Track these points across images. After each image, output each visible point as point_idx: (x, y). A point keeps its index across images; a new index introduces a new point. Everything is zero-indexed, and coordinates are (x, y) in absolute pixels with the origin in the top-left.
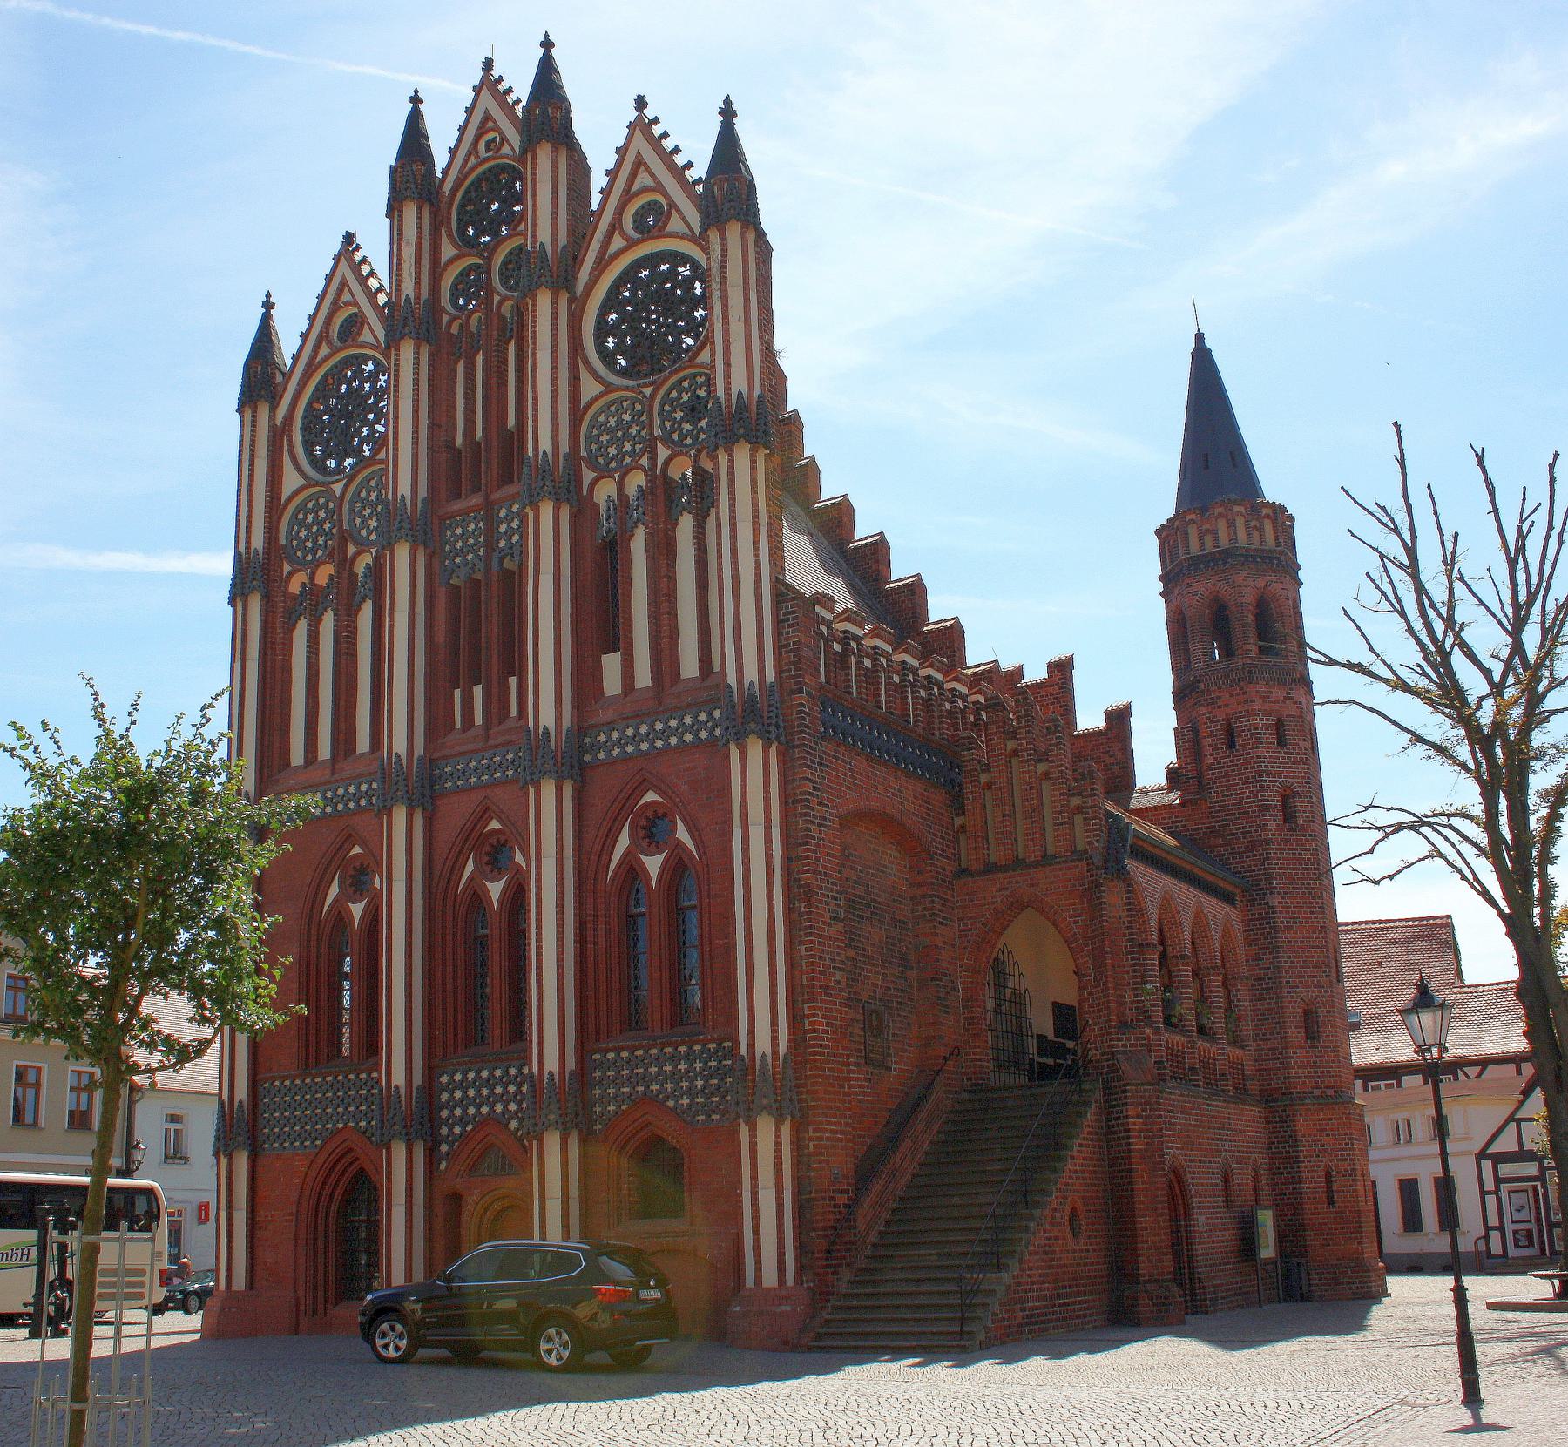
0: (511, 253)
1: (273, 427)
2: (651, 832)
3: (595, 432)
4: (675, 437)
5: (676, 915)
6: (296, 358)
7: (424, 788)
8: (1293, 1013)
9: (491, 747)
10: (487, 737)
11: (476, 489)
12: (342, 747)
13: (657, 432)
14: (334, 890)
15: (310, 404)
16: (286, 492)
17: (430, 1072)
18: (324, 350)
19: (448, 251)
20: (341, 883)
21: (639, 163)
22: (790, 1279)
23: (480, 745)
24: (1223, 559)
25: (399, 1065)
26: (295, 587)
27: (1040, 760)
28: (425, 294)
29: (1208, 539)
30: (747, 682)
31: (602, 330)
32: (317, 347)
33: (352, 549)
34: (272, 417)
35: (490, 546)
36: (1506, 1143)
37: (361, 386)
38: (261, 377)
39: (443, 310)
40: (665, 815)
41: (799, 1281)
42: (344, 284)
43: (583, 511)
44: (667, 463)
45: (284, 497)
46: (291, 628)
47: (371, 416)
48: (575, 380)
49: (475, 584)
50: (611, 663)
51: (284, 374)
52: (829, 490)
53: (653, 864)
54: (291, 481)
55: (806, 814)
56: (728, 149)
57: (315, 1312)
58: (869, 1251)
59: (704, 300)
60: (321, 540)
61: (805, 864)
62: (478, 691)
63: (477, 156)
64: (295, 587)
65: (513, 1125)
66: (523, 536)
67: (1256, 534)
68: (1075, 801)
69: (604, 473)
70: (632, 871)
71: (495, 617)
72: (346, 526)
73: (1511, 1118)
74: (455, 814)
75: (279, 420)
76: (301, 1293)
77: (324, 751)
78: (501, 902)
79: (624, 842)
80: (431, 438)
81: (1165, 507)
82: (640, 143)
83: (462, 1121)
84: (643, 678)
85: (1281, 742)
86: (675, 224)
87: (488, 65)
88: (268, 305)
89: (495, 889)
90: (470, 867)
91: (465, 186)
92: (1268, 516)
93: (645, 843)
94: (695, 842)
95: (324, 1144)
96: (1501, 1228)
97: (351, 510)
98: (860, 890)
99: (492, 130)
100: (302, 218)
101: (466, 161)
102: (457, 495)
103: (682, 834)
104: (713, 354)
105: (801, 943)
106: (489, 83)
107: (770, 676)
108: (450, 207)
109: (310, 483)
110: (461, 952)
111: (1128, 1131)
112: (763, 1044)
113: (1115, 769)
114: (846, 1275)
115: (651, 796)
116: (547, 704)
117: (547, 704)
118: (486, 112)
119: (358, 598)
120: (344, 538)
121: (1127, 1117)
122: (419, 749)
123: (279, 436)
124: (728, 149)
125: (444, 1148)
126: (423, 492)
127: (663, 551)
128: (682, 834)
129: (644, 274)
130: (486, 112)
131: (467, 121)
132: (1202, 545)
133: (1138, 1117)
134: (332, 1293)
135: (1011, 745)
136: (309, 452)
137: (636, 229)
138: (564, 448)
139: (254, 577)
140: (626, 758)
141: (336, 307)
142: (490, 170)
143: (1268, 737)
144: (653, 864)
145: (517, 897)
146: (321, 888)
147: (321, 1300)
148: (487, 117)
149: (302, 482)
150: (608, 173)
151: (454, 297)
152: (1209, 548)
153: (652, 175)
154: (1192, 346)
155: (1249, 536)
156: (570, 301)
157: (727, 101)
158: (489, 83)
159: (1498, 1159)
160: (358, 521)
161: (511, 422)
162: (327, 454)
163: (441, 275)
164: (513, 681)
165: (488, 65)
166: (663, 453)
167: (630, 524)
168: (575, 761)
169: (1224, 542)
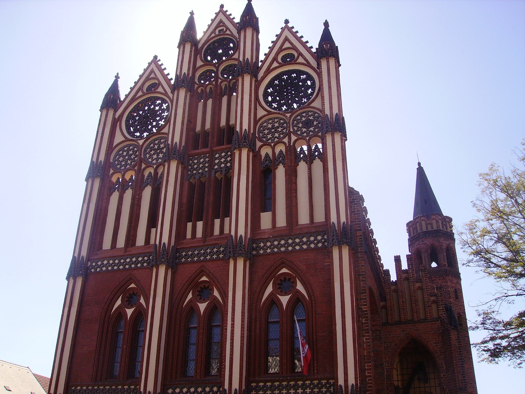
0: (226, 66)
1: (114, 118)
2: (284, 284)
3: (262, 129)
6: (127, 96)
9: (207, 245)
10: (205, 241)
11: (206, 146)
14: (119, 302)
15: (130, 112)
16: (116, 142)
18: (140, 94)
19: (199, 63)
23: (202, 244)
26: (114, 179)
27: (417, 282)
28: (190, 75)
29: (429, 226)
30: (342, 222)
31: (266, 95)
32: (137, 92)
33: (143, 166)
35: (211, 167)
37: (154, 108)
40: (289, 279)
43: (256, 155)
44: (295, 141)
46: (110, 194)
47: (158, 119)
48: (256, 109)
51: (120, 101)
53: (284, 300)
54: (118, 138)
55: (364, 281)
56: (326, 37)
60: (129, 162)
61: (364, 302)
63: (215, 34)
64: (114, 179)
66: (232, 161)
69: (265, 144)
72: (142, 157)
75: (117, 117)
82: (287, 33)
88: (117, 77)
90: (190, 296)
97: (145, 151)
101: (211, 35)
102: (196, 147)
103: (300, 287)
105: (363, 336)
109: (127, 140)
119: (144, 184)
120: (141, 161)
122: (172, 244)
123: (116, 122)
124: (326, 37)
128: (300, 287)
131: (211, 24)
132: (427, 228)
140: (273, 253)
141: (148, 79)
151: (200, 79)
155: (443, 227)
156: (256, 81)
160: (148, 156)
162: (136, 131)
163: (196, 71)
165: (222, 6)
166: (294, 138)
167: (277, 163)
169: (435, 228)
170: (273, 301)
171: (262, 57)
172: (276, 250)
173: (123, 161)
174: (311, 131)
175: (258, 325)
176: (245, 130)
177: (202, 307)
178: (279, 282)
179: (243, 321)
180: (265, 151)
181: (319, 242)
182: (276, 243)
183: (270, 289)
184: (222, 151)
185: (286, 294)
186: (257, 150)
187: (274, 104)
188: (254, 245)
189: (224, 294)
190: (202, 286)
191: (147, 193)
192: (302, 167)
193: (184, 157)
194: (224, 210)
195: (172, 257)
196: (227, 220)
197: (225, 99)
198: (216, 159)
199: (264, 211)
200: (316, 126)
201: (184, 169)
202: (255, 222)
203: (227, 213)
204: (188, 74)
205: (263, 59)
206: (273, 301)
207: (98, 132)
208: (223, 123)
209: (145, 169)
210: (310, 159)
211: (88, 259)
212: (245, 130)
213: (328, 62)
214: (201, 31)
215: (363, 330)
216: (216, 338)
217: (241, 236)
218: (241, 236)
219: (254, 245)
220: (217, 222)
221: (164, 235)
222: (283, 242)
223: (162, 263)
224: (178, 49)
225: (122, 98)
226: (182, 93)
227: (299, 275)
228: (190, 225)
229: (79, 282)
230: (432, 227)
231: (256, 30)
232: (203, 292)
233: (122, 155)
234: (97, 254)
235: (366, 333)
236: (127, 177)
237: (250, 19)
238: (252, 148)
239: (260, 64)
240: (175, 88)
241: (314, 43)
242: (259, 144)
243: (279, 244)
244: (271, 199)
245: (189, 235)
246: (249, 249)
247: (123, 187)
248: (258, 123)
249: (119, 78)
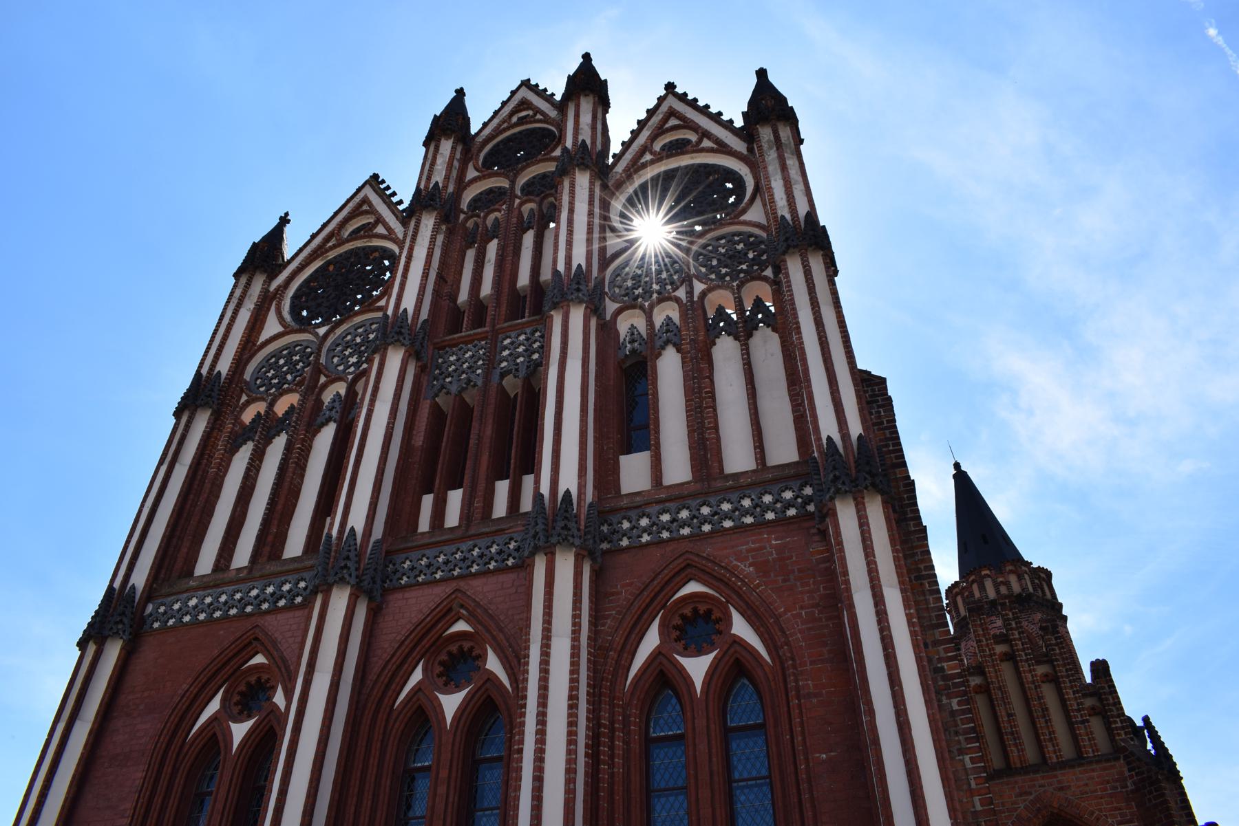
2: (698, 626)
12: (267, 549)
14: (214, 706)
16: (264, 336)
20: (223, 701)
26: (248, 417)
32: (327, 240)
33: (323, 379)
38: (264, 256)
43: (607, 330)
44: (704, 294)
45: (262, 338)
46: (233, 449)
53: (697, 667)
71: (491, 421)
72: (323, 360)
74: (410, 608)
77: (242, 556)
90: (417, 676)
103: (741, 628)
105: (962, 752)
108: (480, 150)
119: (320, 420)
128: (741, 628)
149: (281, 329)
163: (465, 188)
166: (699, 287)
170: (663, 676)
171: (615, 148)
172: (665, 535)
173: (274, 377)
174: (742, 271)
176: (579, 266)
177: (450, 703)
178: (677, 621)
180: (630, 323)
181: (789, 505)
182: (665, 518)
183: (651, 641)
184: (521, 329)
185: (699, 652)
186: (608, 318)
188: (605, 528)
189: (515, 662)
190: (454, 648)
191: (325, 438)
192: (725, 350)
193: (425, 341)
194: (519, 450)
195: (372, 572)
196: (528, 480)
197: (529, 239)
198: (505, 348)
199: (628, 451)
200: (753, 259)
201: (422, 370)
202: (607, 475)
203: (530, 464)
204: (445, 187)
205: (617, 152)
206: (663, 676)
208: (524, 279)
209: (325, 386)
210: (743, 331)
212: (579, 266)
214: (479, 115)
215: (957, 733)
216: (490, 797)
217: (568, 492)
218: (568, 492)
219: (605, 528)
220: (502, 488)
221: (358, 511)
222: (684, 514)
223: (342, 581)
224: (424, 149)
225: (288, 252)
226: (428, 223)
227: (740, 596)
228: (428, 501)
229: (113, 652)
231: (603, 102)
232: (456, 663)
233: (276, 366)
235: (968, 740)
236: (281, 408)
237: (588, 84)
238: (595, 309)
239: (611, 160)
240: (409, 216)
241: (735, 111)
242: (611, 307)
243: (673, 520)
244: (647, 427)
245: (424, 525)
246: (592, 528)
247: (266, 428)
248: (608, 265)
249: (288, 221)
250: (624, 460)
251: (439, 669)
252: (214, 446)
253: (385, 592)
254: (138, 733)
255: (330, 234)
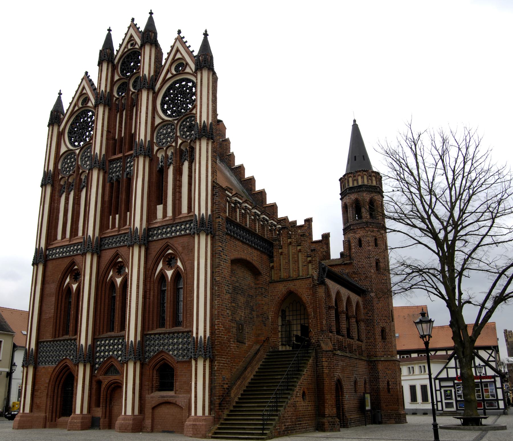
2: (170, 262)
4: (184, 137)
5: (176, 290)
6: (68, 110)
7: (97, 247)
8: (378, 331)
11: (120, 152)
12: (73, 234)
13: (178, 134)
14: (68, 280)
17: (94, 340)
20: (70, 278)
21: (178, 50)
22: (207, 413)
23: (117, 233)
24: (359, 188)
25: (84, 338)
27: (298, 246)
28: (108, 90)
34: (59, 129)
36: (443, 375)
38: (56, 116)
39: (114, 96)
41: (210, 413)
42: (84, 88)
46: (61, 196)
47: (90, 129)
48: (153, 118)
49: (118, 181)
50: (160, 208)
52: (237, 163)
53: (169, 273)
55: (219, 258)
56: (205, 46)
57: (52, 421)
58: (234, 404)
59: (195, 94)
60: (72, 168)
62: (117, 216)
65: (120, 359)
67: (370, 181)
68: (309, 259)
70: (163, 276)
72: (79, 163)
73: (445, 367)
76: (47, 414)
78: (120, 284)
79: (160, 266)
80: (107, 135)
81: (342, 171)
82: (178, 44)
83: (103, 357)
84: (170, 213)
85: (376, 245)
86: (188, 70)
87: (133, 20)
89: (119, 280)
90: (111, 273)
91: (123, 57)
92: (374, 176)
93: (167, 267)
94: (183, 266)
95: (58, 365)
96: (441, 401)
97: (81, 158)
98: (237, 284)
99: (133, 40)
100: (72, 67)
101: (124, 50)
102: (115, 154)
103: (179, 264)
104: (196, 111)
105: (215, 300)
106: (133, 25)
107: (209, 212)
108: (118, 66)
110: (107, 300)
111: (323, 366)
112: (201, 334)
113: (324, 253)
114: (226, 412)
115: (170, 251)
116: (138, 220)
117: (138, 220)
118: (131, 34)
121: (323, 362)
122: (97, 234)
123: (60, 135)
124: (205, 46)
125: (97, 366)
126: (103, 152)
127: (178, 173)
128: (179, 264)
129: (177, 85)
130: (131, 34)
131: (125, 37)
133: (326, 362)
134: (58, 414)
135: (289, 240)
136: (70, 140)
137: (176, 71)
138: (148, 139)
139: (49, 179)
142: (131, 52)
143: (372, 243)
144: (169, 273)
145: (125, 283)
146: (63, 279)
147: (54, 416)
148: (131, 36)
150: (168, 53)
152: (356, 185)
153: (181, 54)
154: (352, 123)
155: (368, 181)
157: (206, 31)
158: (133, 25)
159: (441, 380)
161: (133, 131)
163: (114, 85)
164: (128, 213)
168: (146, 239)
173: (67, 167)
175: (152, 293)
179: (138, 292)
185: (171, 269)
187: (168, 111)
202: (151, 214)
207: (47, 145)
211: (46, 249)
213: (202, 73)
230: (358, 183)
234: (52, 244)
250: (158, 206)
251: (117, 270)
252: (55, 196)
253: (101, 251)
254: (52, 288)
255: (74, 104)
